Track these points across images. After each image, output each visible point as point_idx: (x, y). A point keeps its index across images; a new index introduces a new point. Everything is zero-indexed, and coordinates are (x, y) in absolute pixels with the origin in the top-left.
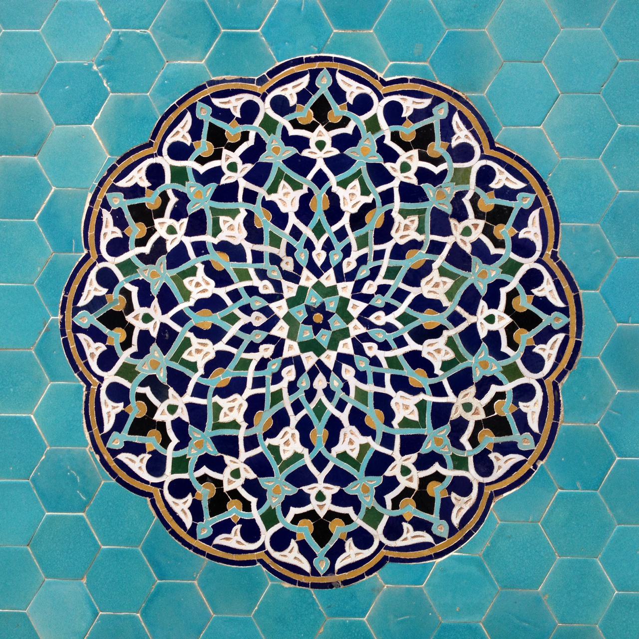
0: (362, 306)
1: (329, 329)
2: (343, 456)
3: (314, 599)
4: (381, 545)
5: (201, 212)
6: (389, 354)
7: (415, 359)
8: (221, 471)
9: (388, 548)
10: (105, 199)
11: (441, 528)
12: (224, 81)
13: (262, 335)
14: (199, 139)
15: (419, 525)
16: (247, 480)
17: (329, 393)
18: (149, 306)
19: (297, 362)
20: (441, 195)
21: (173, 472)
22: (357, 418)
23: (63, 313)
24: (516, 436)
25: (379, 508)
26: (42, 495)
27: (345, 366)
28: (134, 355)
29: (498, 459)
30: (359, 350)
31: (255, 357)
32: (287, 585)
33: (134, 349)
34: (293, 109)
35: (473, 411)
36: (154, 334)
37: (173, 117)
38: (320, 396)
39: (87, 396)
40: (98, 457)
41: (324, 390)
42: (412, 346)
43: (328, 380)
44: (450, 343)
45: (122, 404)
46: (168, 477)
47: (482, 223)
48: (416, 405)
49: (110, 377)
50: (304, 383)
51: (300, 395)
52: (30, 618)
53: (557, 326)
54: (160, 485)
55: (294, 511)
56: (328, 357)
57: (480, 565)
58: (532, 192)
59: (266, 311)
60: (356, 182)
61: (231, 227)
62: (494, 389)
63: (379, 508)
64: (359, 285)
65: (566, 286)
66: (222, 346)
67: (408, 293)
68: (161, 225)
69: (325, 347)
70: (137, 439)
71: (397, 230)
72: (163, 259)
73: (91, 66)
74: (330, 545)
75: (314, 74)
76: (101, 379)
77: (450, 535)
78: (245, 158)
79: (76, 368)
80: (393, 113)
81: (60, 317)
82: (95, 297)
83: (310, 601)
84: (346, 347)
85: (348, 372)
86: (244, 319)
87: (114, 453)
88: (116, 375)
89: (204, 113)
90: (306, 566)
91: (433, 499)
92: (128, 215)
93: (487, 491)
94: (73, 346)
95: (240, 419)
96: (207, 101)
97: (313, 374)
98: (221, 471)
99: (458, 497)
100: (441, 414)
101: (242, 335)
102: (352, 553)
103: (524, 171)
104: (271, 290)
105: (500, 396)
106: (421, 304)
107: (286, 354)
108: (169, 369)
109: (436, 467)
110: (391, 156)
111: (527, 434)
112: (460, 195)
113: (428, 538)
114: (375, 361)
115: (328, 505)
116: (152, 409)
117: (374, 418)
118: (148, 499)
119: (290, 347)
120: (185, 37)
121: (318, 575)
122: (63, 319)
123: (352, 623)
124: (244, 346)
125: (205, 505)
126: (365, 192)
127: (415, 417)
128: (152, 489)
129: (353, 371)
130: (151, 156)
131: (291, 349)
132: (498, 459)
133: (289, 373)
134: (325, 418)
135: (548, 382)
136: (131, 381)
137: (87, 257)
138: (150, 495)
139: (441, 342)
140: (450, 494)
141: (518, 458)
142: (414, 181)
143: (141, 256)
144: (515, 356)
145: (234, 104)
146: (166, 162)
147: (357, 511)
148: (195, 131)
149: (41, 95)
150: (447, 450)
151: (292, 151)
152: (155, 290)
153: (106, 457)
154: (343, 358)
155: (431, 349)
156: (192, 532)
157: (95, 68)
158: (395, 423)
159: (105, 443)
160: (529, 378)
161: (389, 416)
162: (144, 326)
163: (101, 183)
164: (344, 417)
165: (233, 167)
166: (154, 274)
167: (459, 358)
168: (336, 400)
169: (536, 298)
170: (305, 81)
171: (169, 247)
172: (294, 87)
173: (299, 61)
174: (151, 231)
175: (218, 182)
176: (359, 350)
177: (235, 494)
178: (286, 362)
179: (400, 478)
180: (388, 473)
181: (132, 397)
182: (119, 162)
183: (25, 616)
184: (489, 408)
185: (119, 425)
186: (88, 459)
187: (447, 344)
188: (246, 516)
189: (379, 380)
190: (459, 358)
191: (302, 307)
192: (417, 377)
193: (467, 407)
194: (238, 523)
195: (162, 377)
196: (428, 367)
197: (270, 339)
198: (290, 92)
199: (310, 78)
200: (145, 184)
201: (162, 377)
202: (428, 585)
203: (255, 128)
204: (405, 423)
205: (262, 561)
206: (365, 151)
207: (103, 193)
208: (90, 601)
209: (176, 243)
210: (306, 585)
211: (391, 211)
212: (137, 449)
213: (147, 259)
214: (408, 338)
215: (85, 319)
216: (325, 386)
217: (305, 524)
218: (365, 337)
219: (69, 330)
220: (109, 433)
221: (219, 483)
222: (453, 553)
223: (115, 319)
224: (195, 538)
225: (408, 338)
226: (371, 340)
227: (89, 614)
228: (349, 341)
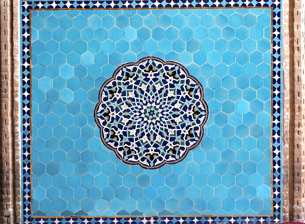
0: (154, 123)
1: (149, 115)
2: (122, 119)
4: (104, 127)
5: (175, 87)
6: (144, 129)
7: (143, 134)
8: (118, 93)
9: (103, 129)
10: (177, 65)
11: (107, 140)
12: (203, 91)
13: (148, 101)
15: (108, 135)
17: (135, 116)
19: (142, 109)
20: (179, 139)
23: (152, 57)
24: (127, 156)
25: (111, 127)
26: (112, 54)
27: (141, 119)
28: (143, 73)
29: (122, 152)
30: (145, 122)
31: (143, 99)
32: (94, 107)
33: (144, 73)
34: (197, 106)
35: (132, 147)
36: (148, 77)
37: (195, 80)
38: (135, 114)
39: (134, 63)
40: (121, 66)
41: (136, 115)
42: (146, 134)
43: (138, 115)
44: (147, 142)
45: (132, 70)
46: (117, 81)
47: (173, 148)
48: (133, 135)
49: (138, 68)
50: (137, 110)
51: (135, 109)
52: (86, 52)
53: (151, 164)
54: (115, 79)
56: (143, 115)
57: (99, 148)
58: (179, 159)
59: (153, 101)
60: (181, 121)
62: (137, 151)
63: (111, 127)
64: (159, 122)
65: (159, 166)
66: (145, 92)
68: (171, 78)
69: (145, 115)
70: (125, 74)
71: (171, 130)
72: (164, 78)
73: (206, 62)
74: (103, 116)
75: (205, 111)
76: (138, 66)
78: (187, 96)
79: (140, 60)
80: (196, 128)
81: (151, 56)
84: (145, 119)
85: (140, 120)
86: (151, 97)
87: (122, 69)
88: (139, 69)
89: (196, 87)
92: (174, 71)
93: (115, 150)
94: (145, 59)
95: (129, 96)
96: (199, 87)
97: (139, 112)
99: (114, 144)
100: (131, 140)
101: (148, 96)
102: (101, 121)
103: (184, 157)
104: (158, 103)
106: (155, 135)
107: (144, 106)
109: (120, 139)
111: (127, 158)
112: (179, 144)
113: (105, 137)
114: (142, 125)
115: (111, 116)
116: (131, 77)
117: (131, 125)
118: (112, 77)
119: (145, 107)
122: (151, 57)
123: (87, 121)
124: (145, 97)
125: (111, 89)
126: (179, 123)
127: (131, 134)
129: (140, 121)
130: (187, 76)
131: (145, 107)
132: (122, 152)
133: (139, 107)
134: (130, 115)
136: (137, 72)
139: (147, 140)
140: (115, 142)
142: (182, 133)
143: (165, 74)
144: (144, 156)
145: (198, 94)
146: (185, 79)
147: (110, 122)
148: (192, 85)
149: (200, 51)
150: (124, 141)
151: (188, 107)
152: (157, 77)
154: (143, 119)
155: (145, 138)
157: (206, 63)
158: (129, 130)
161: (131, 129)
162: (149, 75)
163: (181, 65)
164: (130, 119)
165: (184, 93)
166: (161, 77)
167: (143, 144)
168: (134, 117)
169: (157, 160)
170: (203, 109)
171: (167, 80)
173: (208, 107)
174: (170, 76)
176: (145, 122)
177: (113, 96)
178: (142, 106)
179: (118, 131)
180: (119, 129)
181: (134, 73)
182: (185, 68)
183: (86, 51)
184: (133, 150)
185: (128, 70)
187: (146, 141)
188: (109, 98)
189: (138, 126)
190: (143, 144)
191: (154, 109)
192: (139, 135)
194: (107, 97)
195: (138, 79)
196: (141, 137)
197: (147, 103)
198: (201, 106)
200: (181, 74)
201: (138, 79)
204: (129, 132)
205: (99, 102)
206: (188, 123)
207: (178, 65)
208: (90, 65)
209: (168, 81)
210: (95, 111)
211: (175, 128)
212: (123, 74)
213: (164, 75)
214: (147, 133)
215: (151, 62)
216: (137, 115)
218: (148, 123)
219: (148, 58)
221: (116, 92)
222: (102, 143)
223: (151, 68)
224: (104, 87)
225: (147, 133)
226: (147, 125)
227: (87, 65)
228: (147, 120)
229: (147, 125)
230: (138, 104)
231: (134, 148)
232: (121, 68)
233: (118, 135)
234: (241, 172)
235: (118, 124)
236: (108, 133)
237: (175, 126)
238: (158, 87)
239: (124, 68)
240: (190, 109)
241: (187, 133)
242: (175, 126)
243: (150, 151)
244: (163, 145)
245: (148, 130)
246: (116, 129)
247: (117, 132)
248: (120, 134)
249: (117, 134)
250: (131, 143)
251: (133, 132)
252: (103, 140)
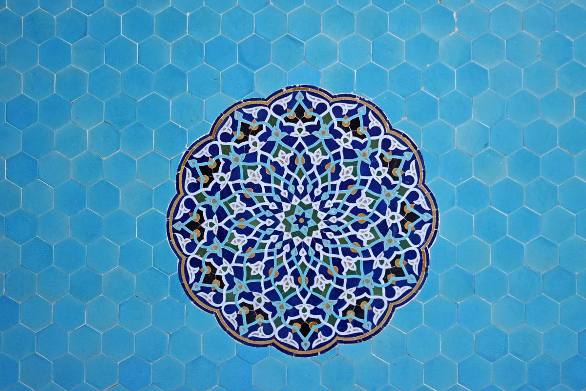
0: (320, 237)
1: (300, 228)
2: (249, 269)
5: (317, 139)
8: (208, 218)
16: (212, 231)
22: (269, 264)
30: (299, 248)
34: (388, 151)
56: (288, 235)
59: (290, 196)
60: (372, 200)
61: (317, 156)
62: (319, 317)
64: (328, 230)
66: (263, 185)
67: (338, 254)
68: (300, 124)
71: (363, 232)
76: (216, 139)
80: (413, 196)
86: (281, 188)
94: (223, 118)
95: (236, 213)
104: (301, 192)
106: (337, 262)
107: (278, 216)
114: (298, 258)
115: (223, 274)
117: (274, 272)
126: (371, 206)
127: (285, 290)
131: (280, 216)
133: (269, 222)
134: (260, 251)
135: (338, 338)
138: (179, 193)
151: (369, 162)
161: (278, 279)
164: (266, 258)
172: (398, 145)
176: (299, 248)
191: (302, 211)
193: (304, 310)
196: (311, 283)
204: (280, 287)
206: (388, 195)
237: (367, 218)
238: (282, 160)
240: (376, 165)
241: (399, 218)
242: (367, 218)
244: (366, 272)
250: (297, 307)
251: (287, 282)
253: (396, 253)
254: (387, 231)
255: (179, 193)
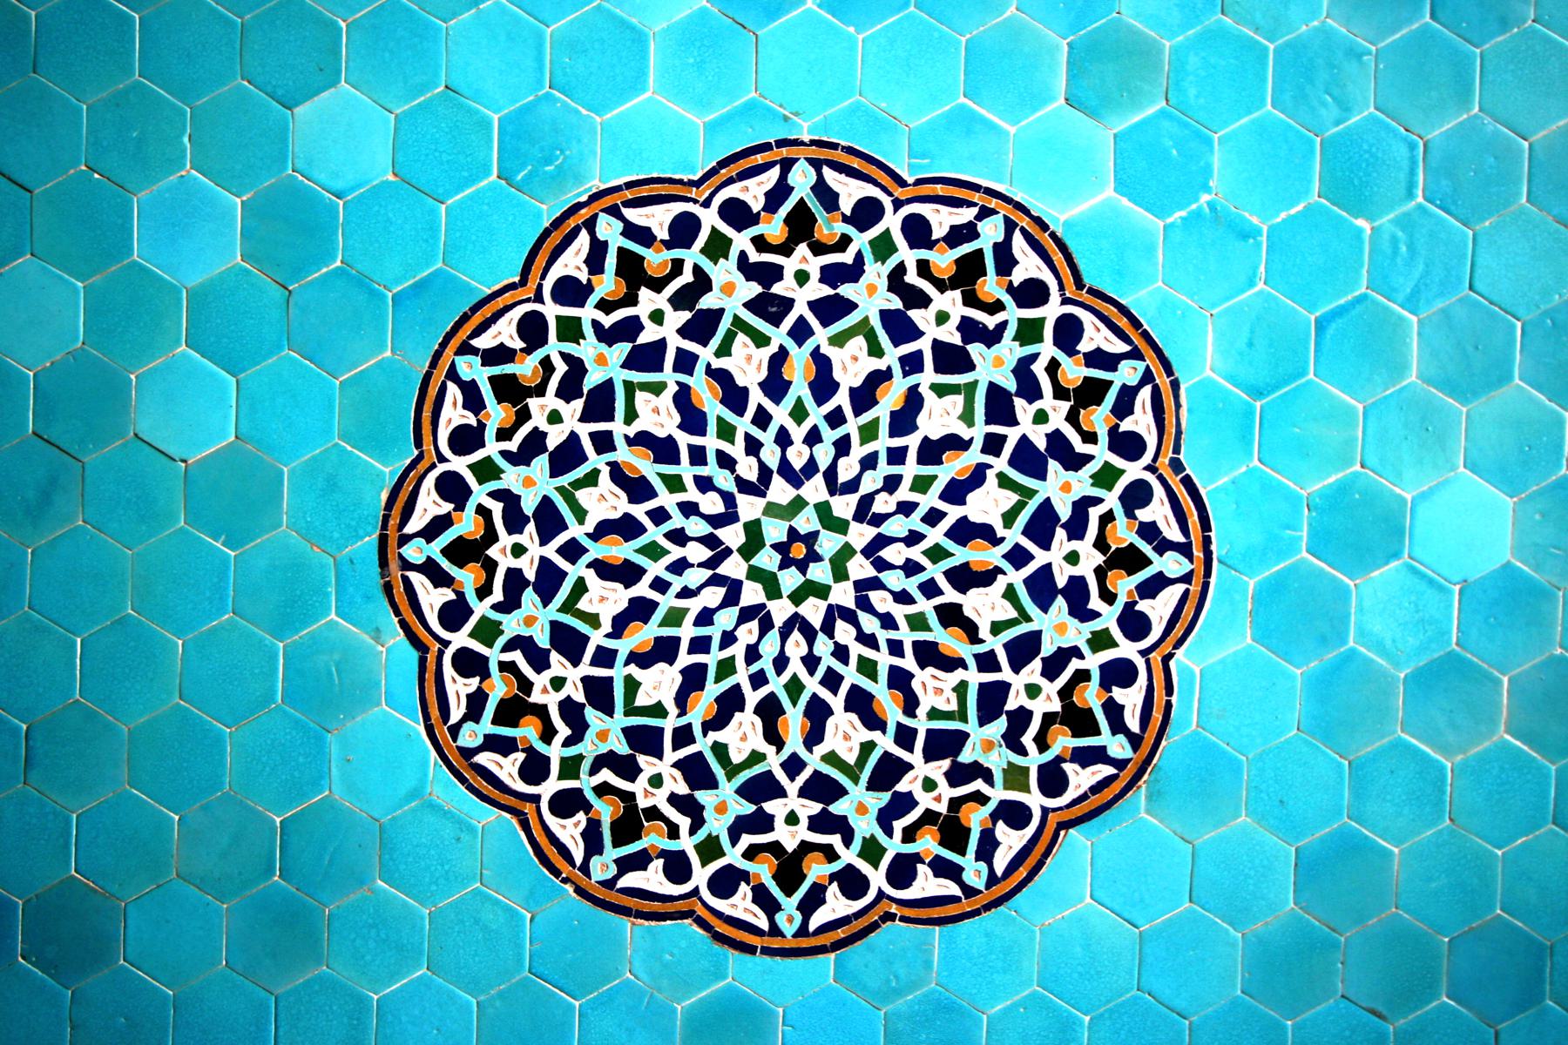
0: (816, 620)
1: (781, 567)
2: (580, 587)
3: (362, 538)
4: (446, 644)
5: (969, 366)
7: (730, 703)
8: (559, 394)
9: (441, 653)
10: (993, 212)
11: (471, 736)
12: (1178, 406)
13: (772, 461)
14: (1088, 365)
15: (476, 702)
16: (545, 435)
17: (680, 566)
18: (821, 281)
19: (728, 517)
20: (988, 746)
21: (558, 318)
22: (640, 610)
23: (813, 143)
24: (611, 853)
25: (501, 642)
28: (743, 256)
29: (577, 824)
30: (746, 615)
31: (737, 450)
32: (384, 496)
34: (1130, 514)
35: (650, 789)
36: (777, 289)
37: (1123, 323)
38: (676, 552)
39: (680, 182)
40: (584, 198)
41: (684, 559)
42: (752, 698)
43: (700, 565)
45: (667, 237)
46: (551, 311)
47: (942, 808)
49: (710, 219)
50: (697, 527)
52: (332, 90)
53: (780, 918)
54: (539, 298)
55: (497, 508)
57: (415, 794)
58: (988, 886)
60: (1013, 614)
62: (684, 822)
63: (501, 642)
64: (849, 616)
65: (841, 933)
67: (835, 693)
68: (951, 302)
69: (754, 562)
70: (611, 261)
72: (896, 303)
73: (1207, 189)
74: (445, 564)
75: (1185, 550)
76: (706, 204)
77: (461, 750)
78: (1056, 438)
79: (723, 164)
80: (1119, 673)
81: (806, 140)
82: (836, 195)
83: (361, 532)
84: (752, 594)
86: (798, 433)
87: (590, 225)
89: (1128, 373)
90: (414, 526)
91: (515, 725)
92: (966, 248)
93: (528, 808)
94: (759, 159)
96: (1148, 377)
97: (710, 541)
98: (559, 394)
99: (518, 764)
101: (773, 429)
102: (432, 598)
103: (1022, 872)
105: (674, 832)
106: (818, 713)
108: (722, 311)
109: (564, 731)
110: (1051, 671)
111: (613, 870)
112: (988, 776)
113: (456, 715)
114: (728, 639)
115: (505, 562)
116: (658, 285)
118: (517, 279)
120: (1250, 344)
121: (400, 545)
122: (803, 143)
123: (327, 595)
124: (756, 432)
125: (508, 369)
126: (997, 628)
127: (642, 700)
128: (532, 285)
130: (1062, 288)
131: (749, 507)
132: (577, 824)
136: (703, 251)
137: (902, 183)
138: (523, 282)
141: (578, 856)
142: (1011, 705)
143: (901, 269)
145: (1141, 421)
146: (1052, 311)
147: (496, 607)
148: (1099, 359)
149: (1162, 112)
150: (589, 748)
152: (846, 290)
153: (583, 211)
154: (734, 591)
156: (466, 349)
157: (1205, 198)
158: (633, 669)
159: (606, 211)
160: (701, 875)
161: (642, 659)
162: (789, 274)
163: (1019, 207)
164: (642, 589)
165: (1041, 418)
166: (872, 289)
168: (668, 577)
169: (823, 889)
170: (1173, 533)
171: (914, 314)
173: (1205, 524)
174: (941, 286)
175: (1018, 394)
176: (746, 615)
177: (524, 416)
178: (729, 499)
179: (547, 675)
180: (555, 657)
181: (677, 253)
182: (1053, 236)
183: (334, 83)
184: (654, 813)
185: (632, 231)
186: (582, 184)
187: (754, 752)
188: (490, 434)
190: (732, 771)
191: (815, 525)
192: (704, 703)
193: (656, 781)
194: (479, 421)
195: (707, 302)
196: (718, 721)
198: (1157, 511)
199: (1179, 544)
200: (1018, 276)
201: (707, 302)
202: (386, 713)
203: (1102, 453)
204: (632, 686)
205: (420, 457)
206: (1061, 629)
207: (1004, 210)
208: (359, 186)
209: (921, 325)
210: (385, 526)
211: (965, 667)
212: (595, 260)
213: (896, 280)
214: (763, 692)
215: (802, 179)
217: (476, 525)
218: (766, 625)
219: (785, 152)
220: (621, 217)
221: (540, 391)
222: (433, 753)
223: (801, 226)
224: (456, 354)
225: (763, 692)
227: (338, 185)
229: (762, 635)
230: (704, 484)
231: (660, 799)
232: (585, 213)
233: (552, 701)
234: (1436, 996)
235: (555, 625)
236: (474, 682)
237: (966, 651)
238: (848, 362)
239: (603, 219)
240: (1076, 529)
241: (1048, 702)
242: (966, 651)
243: (779, 822)
244: (873, 785)
245: (770, 672)
246: (540, 661)
247: (540, 680)
248: (562, 695)
249: (545, 691)
250: (642, 760)
252: (443, 732)
253: (978, 785)
254: (998, 716)
255: (523, 282)
